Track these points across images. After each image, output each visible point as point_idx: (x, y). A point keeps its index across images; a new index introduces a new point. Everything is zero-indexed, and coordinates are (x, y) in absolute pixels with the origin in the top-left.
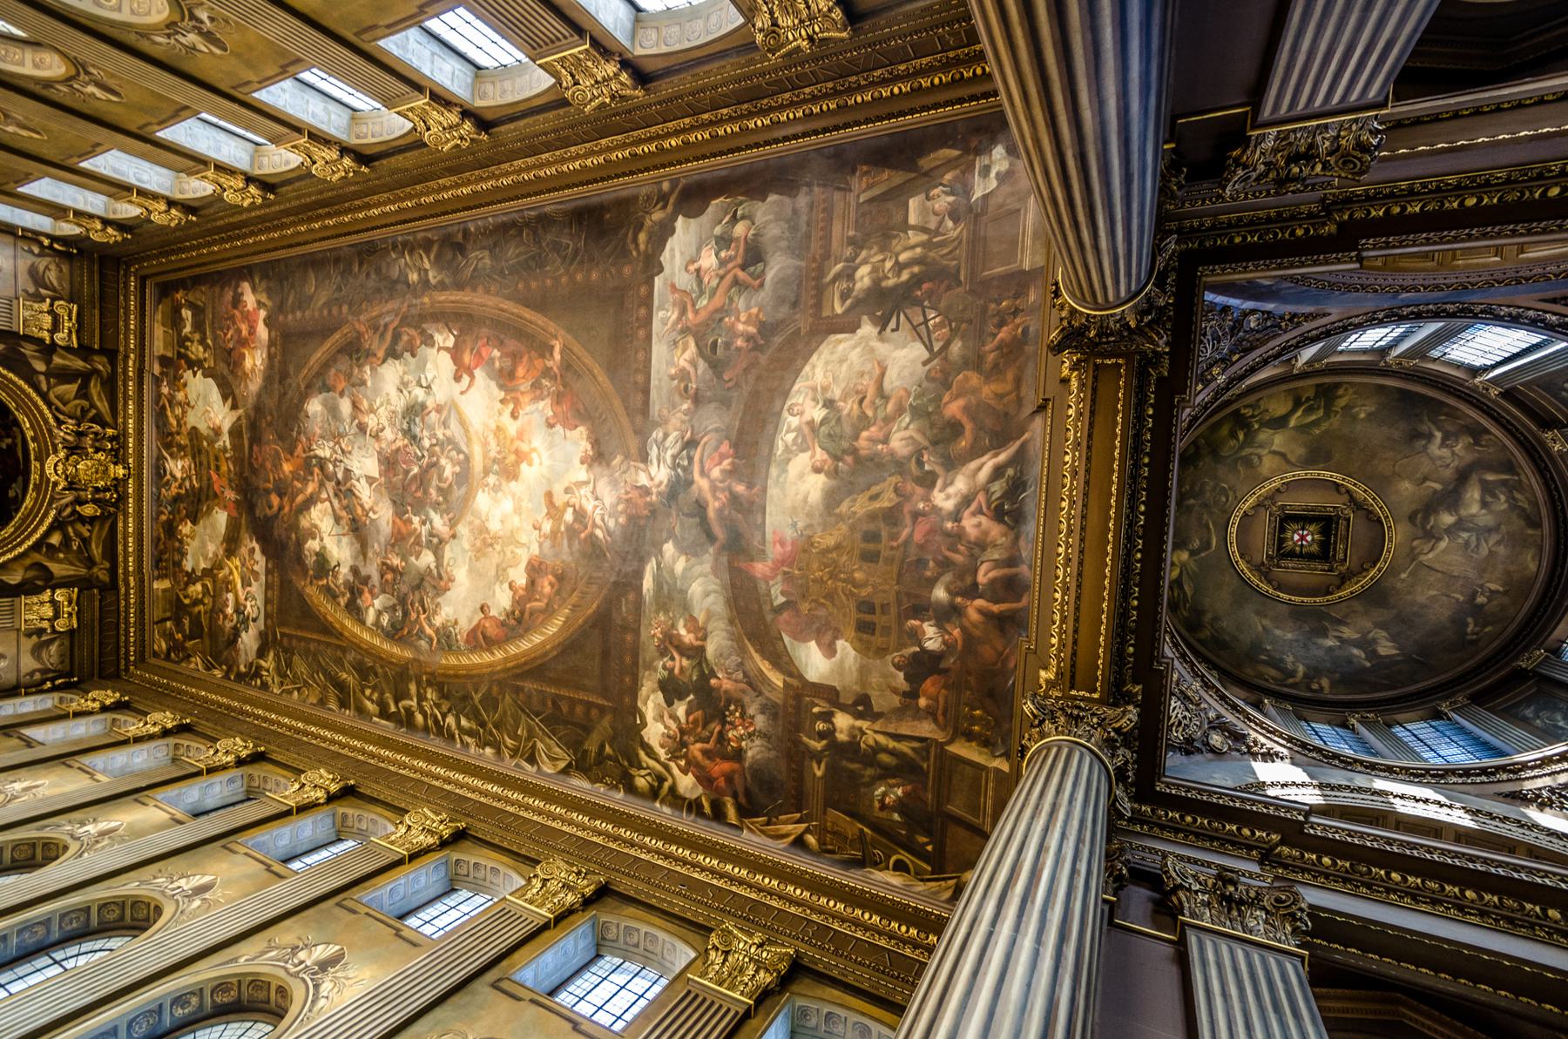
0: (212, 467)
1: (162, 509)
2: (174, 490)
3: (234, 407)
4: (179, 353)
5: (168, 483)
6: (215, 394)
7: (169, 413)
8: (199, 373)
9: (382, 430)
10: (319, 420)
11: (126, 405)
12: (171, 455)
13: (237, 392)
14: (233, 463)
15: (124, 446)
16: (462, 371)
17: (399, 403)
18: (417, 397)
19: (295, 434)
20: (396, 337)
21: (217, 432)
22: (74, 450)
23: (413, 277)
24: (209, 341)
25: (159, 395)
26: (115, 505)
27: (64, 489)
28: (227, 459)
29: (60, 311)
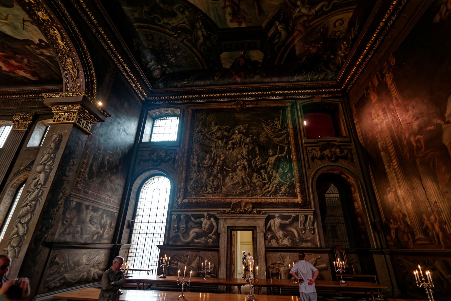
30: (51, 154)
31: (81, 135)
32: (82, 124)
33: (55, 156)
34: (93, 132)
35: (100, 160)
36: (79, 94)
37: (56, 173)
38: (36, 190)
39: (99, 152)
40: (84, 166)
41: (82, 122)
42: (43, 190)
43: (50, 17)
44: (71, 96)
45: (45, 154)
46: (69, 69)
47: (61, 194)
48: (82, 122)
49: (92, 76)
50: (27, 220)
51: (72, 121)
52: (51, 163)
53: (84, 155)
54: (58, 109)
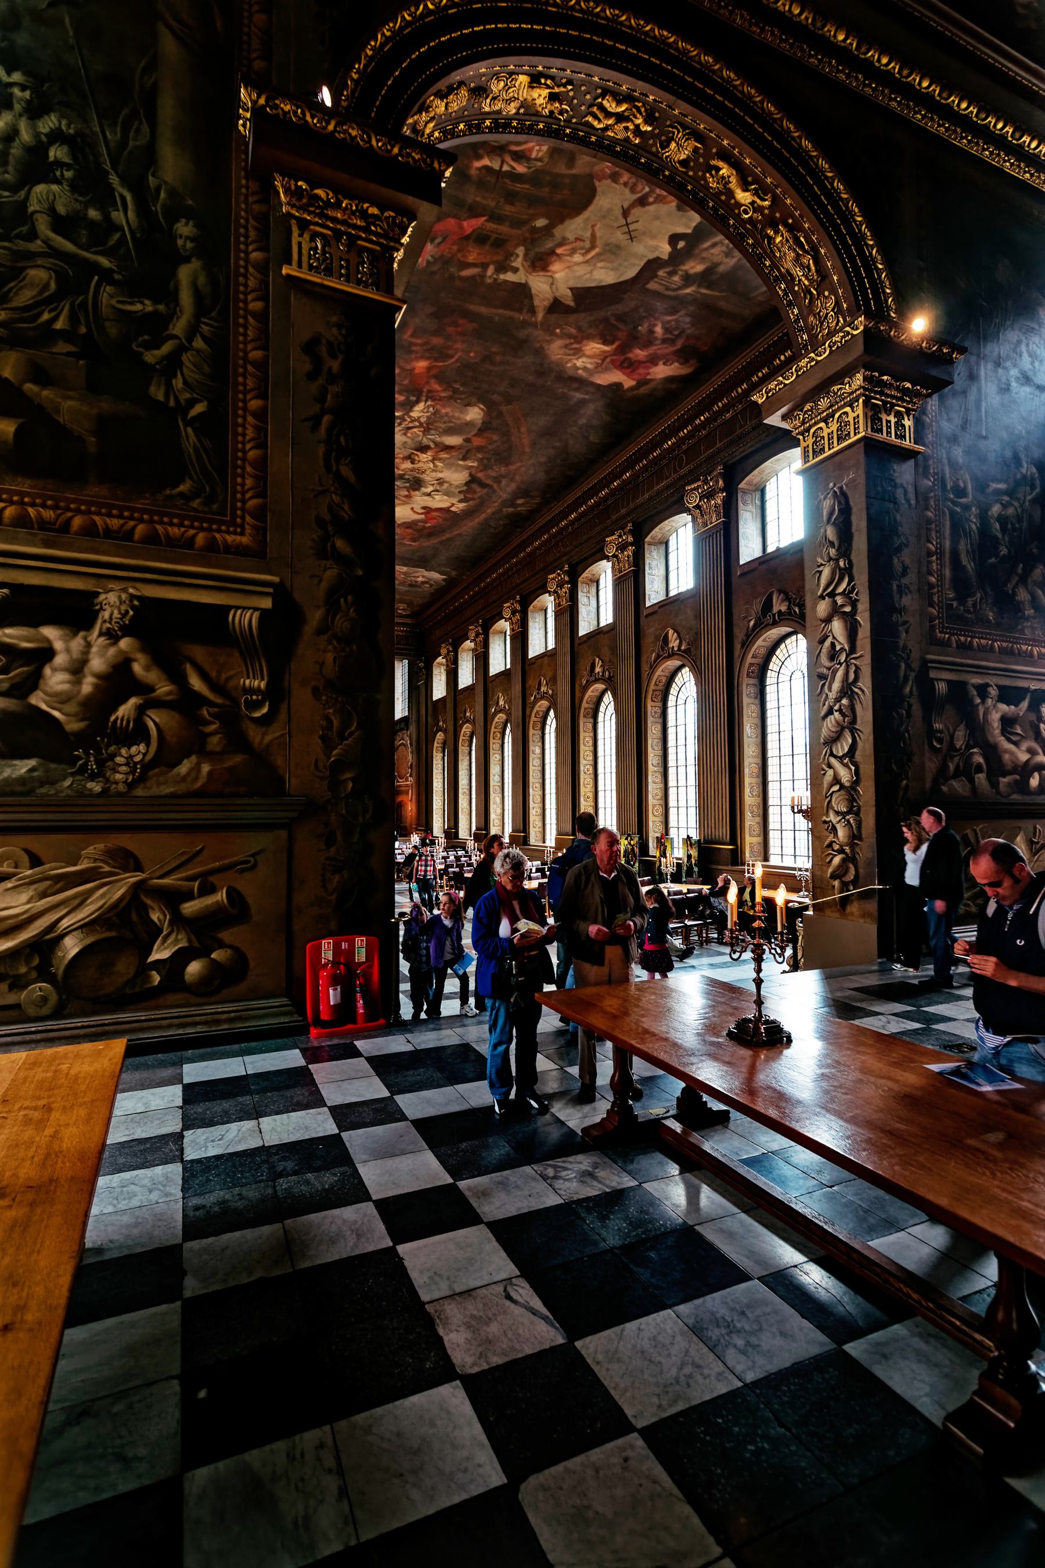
0: (491, 226)
3: (556, 306)
6: (604, 276)
8: (665, 249)
9: (412, 463)
10: (457, 414)
13: (572, 318)
14: (473, 278)
16: (427, 510)
17: (426, 477)
18: (426, 487)
19: (457, 386)
20: (483, 485)
21: (540, 262)
23: (520, 501)
24: (688, 291)
28: (485, 266)
30: (837, 561)
31: (895, 467)
32: (884, 429)
33: (851, 563)
34: (927, 441)
35: (974, 527)
36: (848, 333)
37: (870, 610)
38: (838, 670)
39: (963, 500)
40: (934, 564)
41: (884, 424)
42: (855, 665)
43: (698, 136)
44: (827, 353)
45: (822, 565)
46: (787, 271)
47: (903, 665)
48: (884, 424)
49: (859, 240)
50: (846, 749)
51: (855, 434)
52: (849, 584)
53: (925, 528)
54: (804, 419)
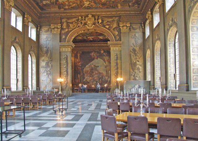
1: (99, 6)
2: (93, 4)
4: (56, 4)
5: (91, 6)
7: (73, 6)
11: (73, 15)
12: (84, 5)
15: (84, 15)
22: (85, 24)
25: (69, 9)
26: (99, 17)
27: (95, 25)
29: (53, 27)
